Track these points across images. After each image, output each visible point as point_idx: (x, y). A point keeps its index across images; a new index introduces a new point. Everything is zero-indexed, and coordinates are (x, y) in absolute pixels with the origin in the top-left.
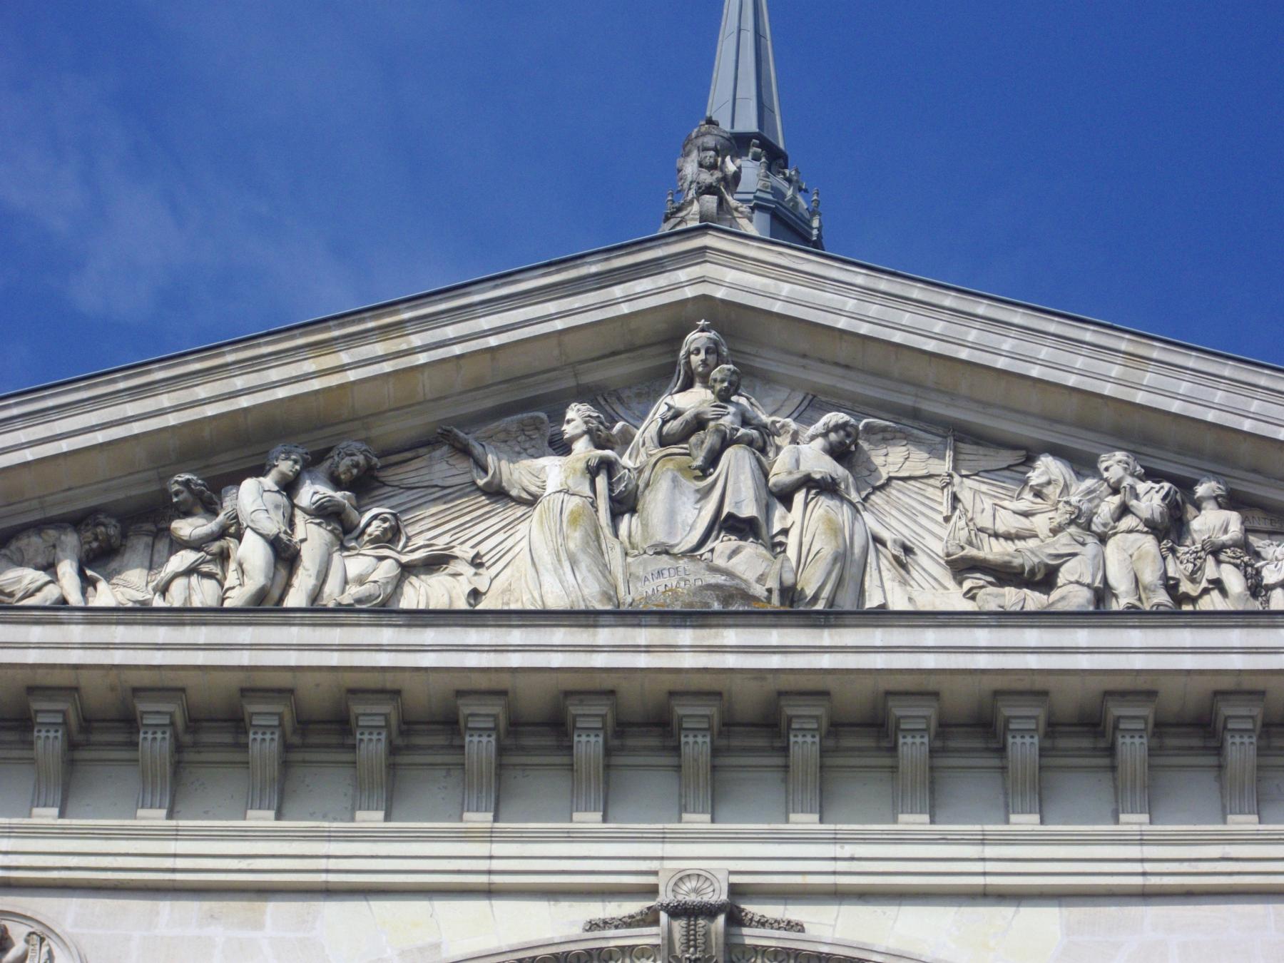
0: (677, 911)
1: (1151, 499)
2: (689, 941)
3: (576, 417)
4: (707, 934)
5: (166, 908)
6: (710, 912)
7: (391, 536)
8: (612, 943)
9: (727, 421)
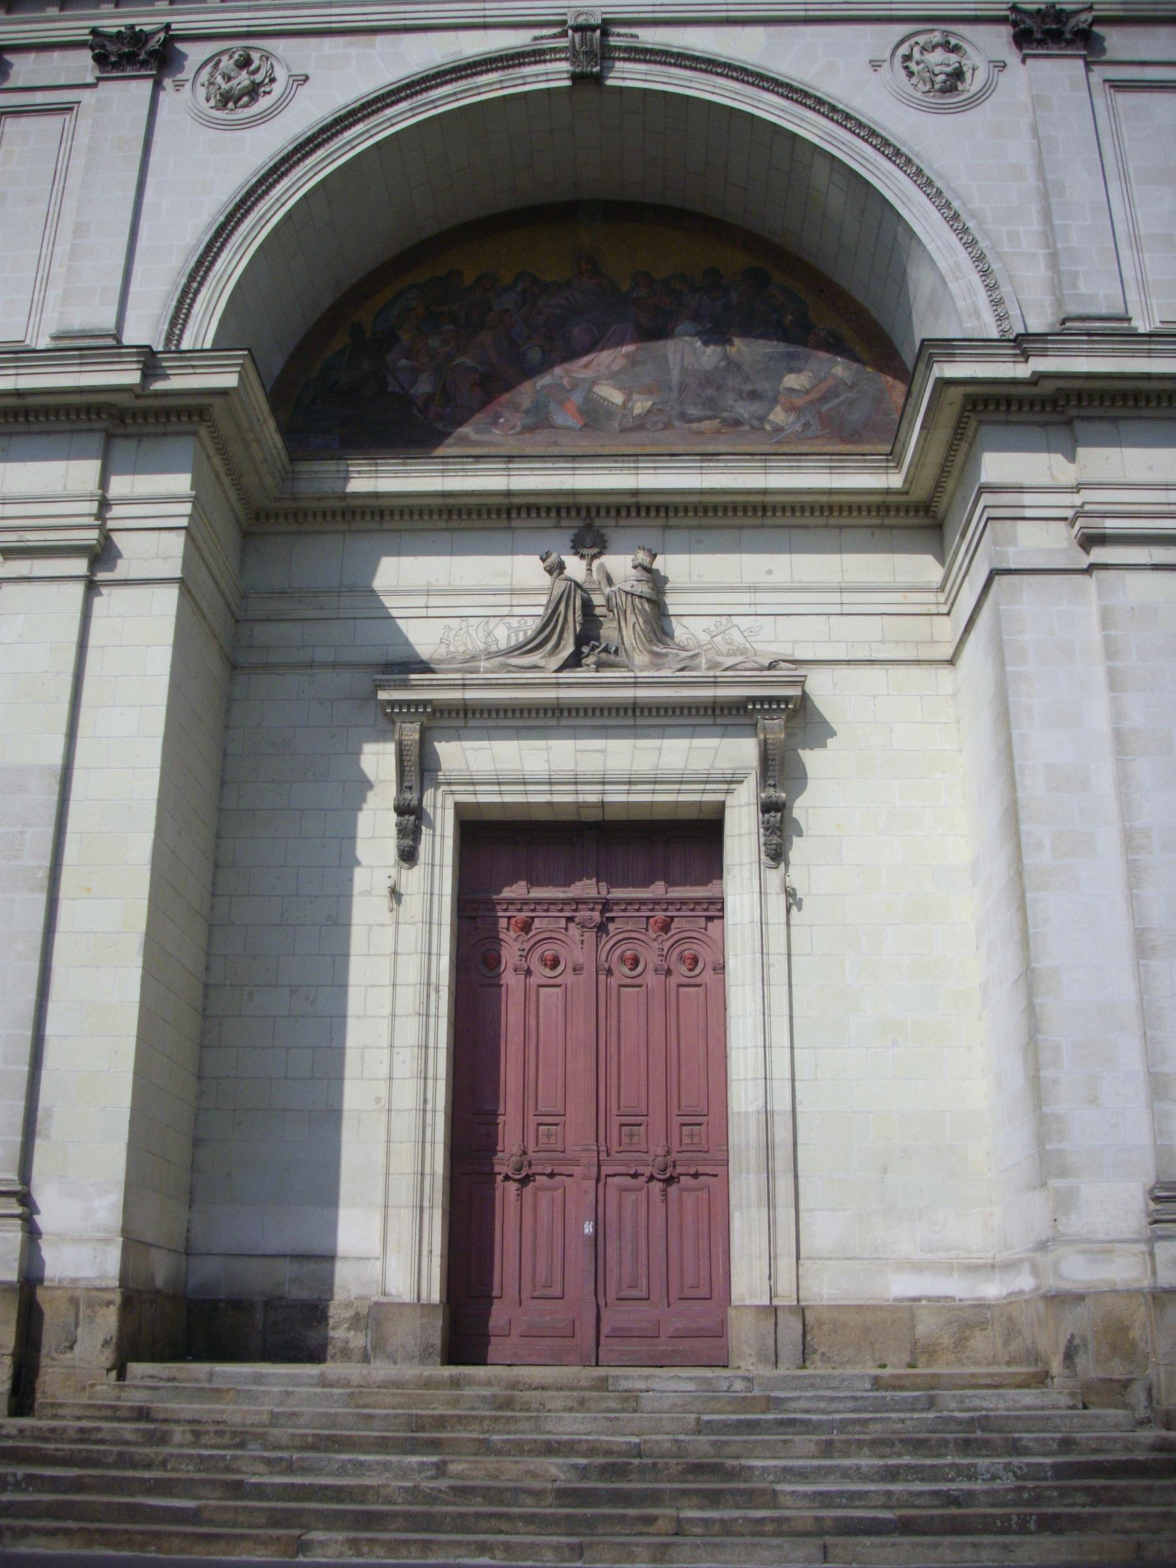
0: (576, 29)
2: (583, 42)
4: (591, 40)
5: (328, 42)
6: (593, 28)
8: (545, 46)
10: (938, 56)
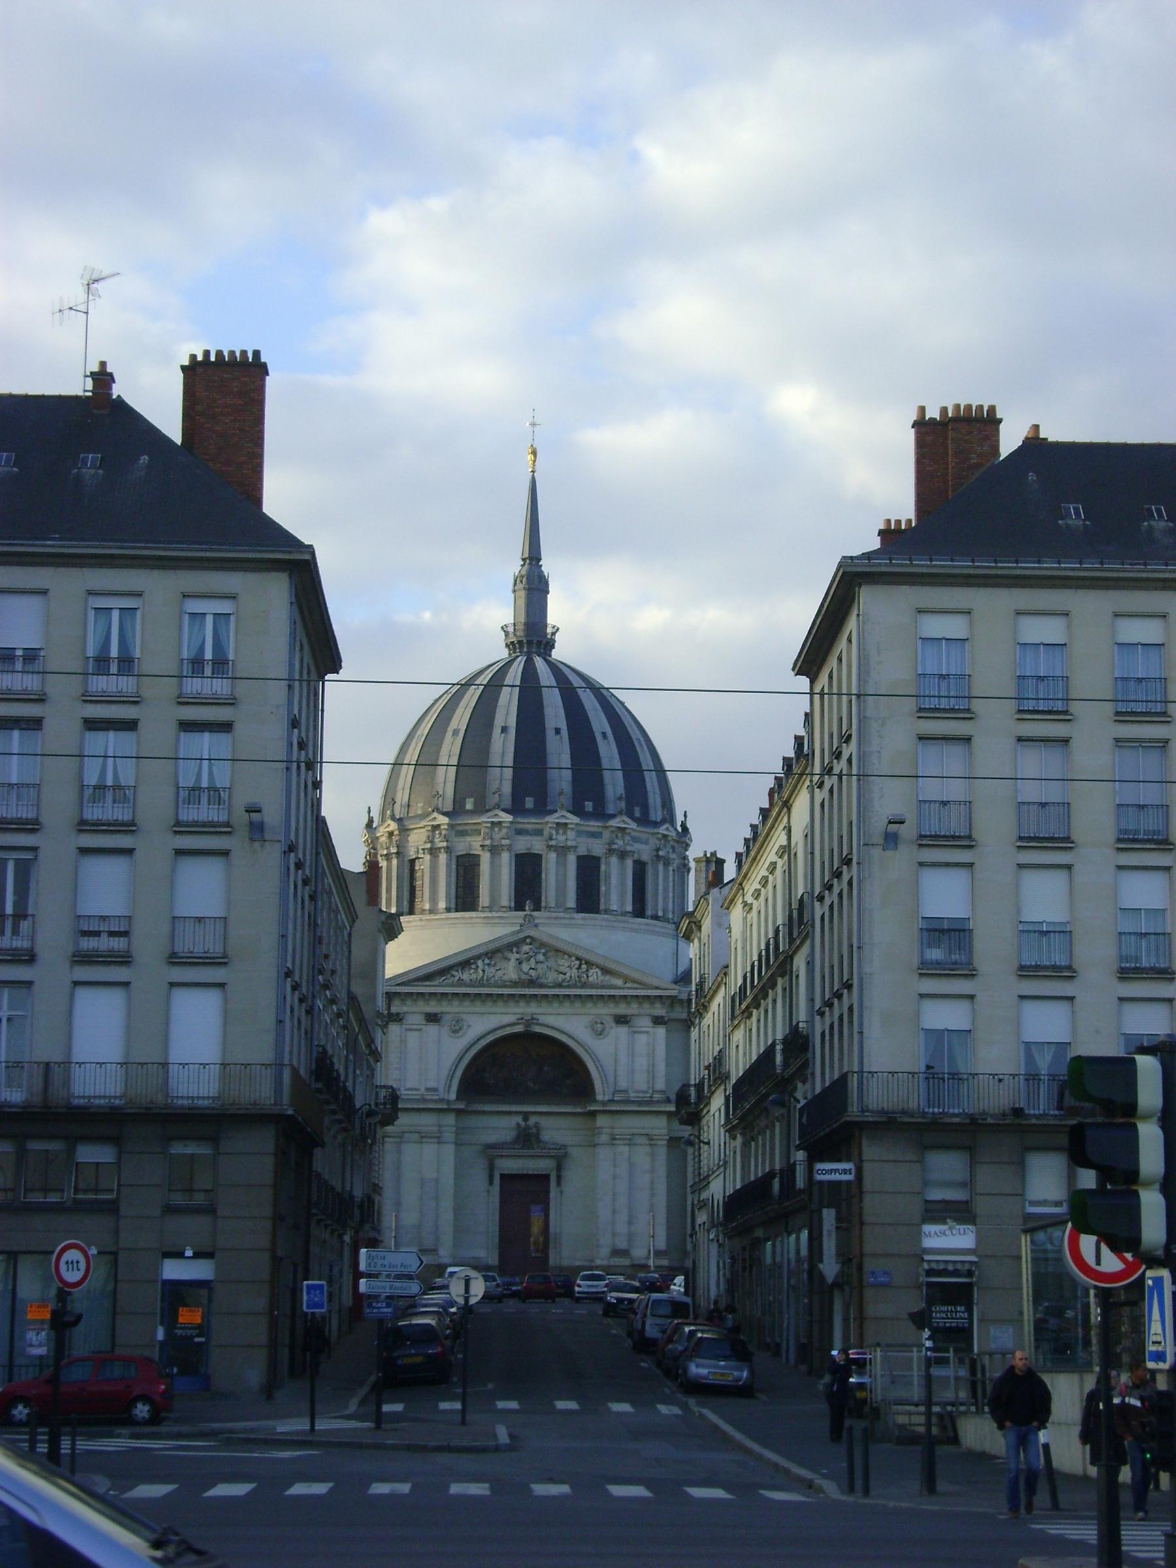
1: (578, 962)
3: (515, 950)
7: (495, 965)
9: (531, 954)
10: (599, 1025)
